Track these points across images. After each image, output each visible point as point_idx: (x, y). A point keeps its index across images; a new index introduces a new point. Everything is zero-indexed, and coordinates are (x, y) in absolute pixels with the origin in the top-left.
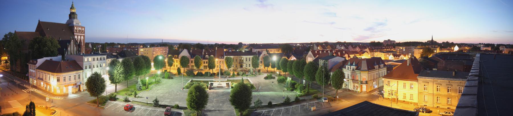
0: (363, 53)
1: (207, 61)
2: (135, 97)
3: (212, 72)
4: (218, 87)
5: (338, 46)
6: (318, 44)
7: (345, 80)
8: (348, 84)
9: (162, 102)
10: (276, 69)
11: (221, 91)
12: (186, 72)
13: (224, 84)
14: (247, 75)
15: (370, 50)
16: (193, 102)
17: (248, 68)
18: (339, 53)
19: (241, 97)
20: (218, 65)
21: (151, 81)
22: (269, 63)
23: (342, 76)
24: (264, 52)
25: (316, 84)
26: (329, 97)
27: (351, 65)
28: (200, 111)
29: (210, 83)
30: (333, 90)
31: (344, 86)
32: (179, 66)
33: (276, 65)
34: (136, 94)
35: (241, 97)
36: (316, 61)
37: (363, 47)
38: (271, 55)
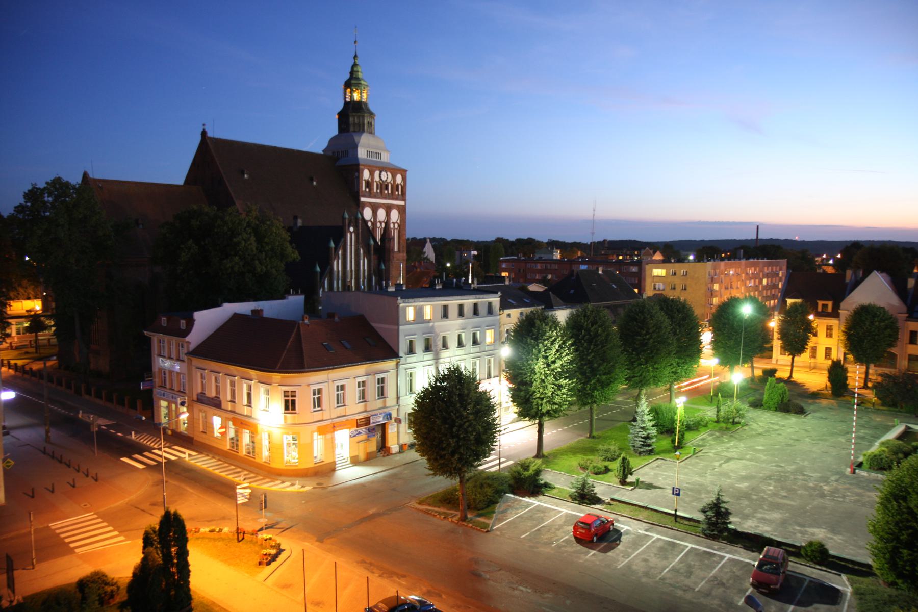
2: (623, 482)
12: (877, 387)
21: (698, 415)
32: (838, 353)
34: (626, 470)
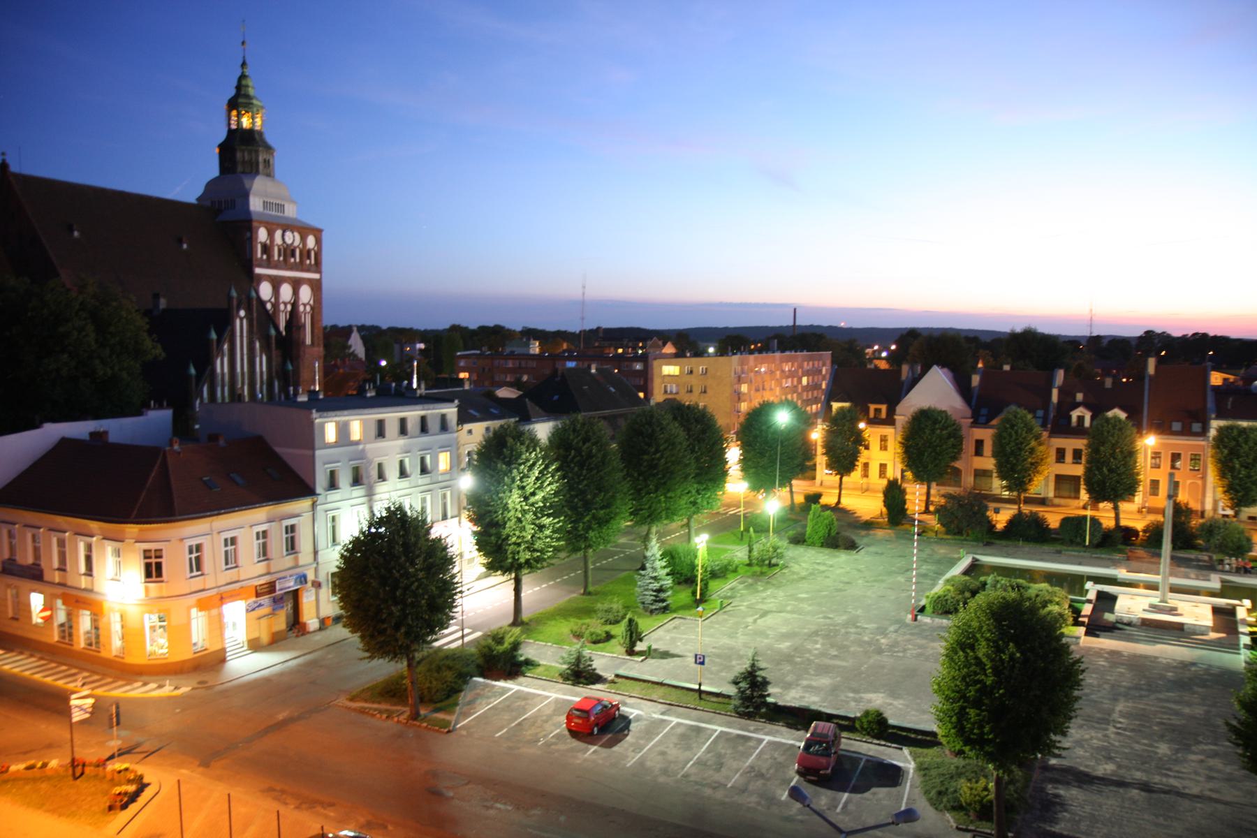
1: (1080, 443)
2: (631, 652)
3: (1108, 521)
4: (1146, 624)
9: (788, 686)
11: (1169, 651)
12: (940, 511)
13: (1196, 612)
16: (977, 704)
20: (1162, 476)
21: (724, 558)
28: (1018, 773)
29: (1092, 589)
32: (894, 471)
34: (634, 635)
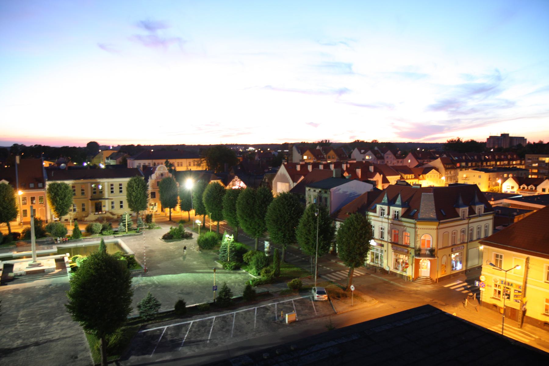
0: (426, 171)
4: (28, 273)
5: (356, 153)
6: (303, 147)
7: (372, 243)
8: (382, 254)
10: (193, 212)
14: (115, 232)
15: (444, 162)
17: (118, 211)
18: (359, 171)
19: (103, 290)
20: (27, 208)
22: (175, 196)
23: (366, 232)
24: (161, 169)
25: (298, 252)
26: (329, 286)
27: (391, 203)
30: (341, 269)
31: (369, 260)
33: (194, 202)
35: (103, 290)
36: (297, 193)
37: (424, 155)
38: (179, 176)
